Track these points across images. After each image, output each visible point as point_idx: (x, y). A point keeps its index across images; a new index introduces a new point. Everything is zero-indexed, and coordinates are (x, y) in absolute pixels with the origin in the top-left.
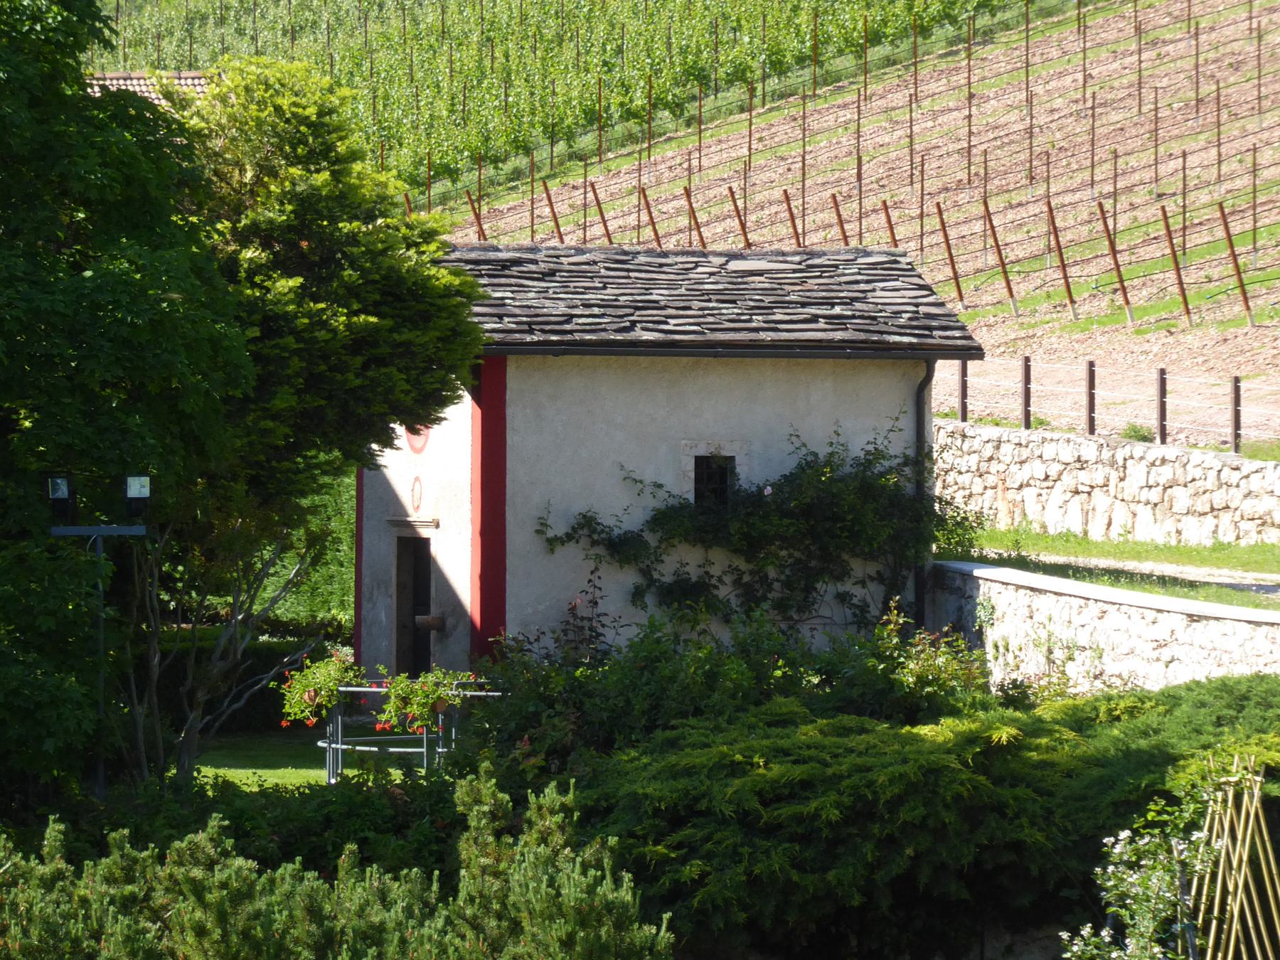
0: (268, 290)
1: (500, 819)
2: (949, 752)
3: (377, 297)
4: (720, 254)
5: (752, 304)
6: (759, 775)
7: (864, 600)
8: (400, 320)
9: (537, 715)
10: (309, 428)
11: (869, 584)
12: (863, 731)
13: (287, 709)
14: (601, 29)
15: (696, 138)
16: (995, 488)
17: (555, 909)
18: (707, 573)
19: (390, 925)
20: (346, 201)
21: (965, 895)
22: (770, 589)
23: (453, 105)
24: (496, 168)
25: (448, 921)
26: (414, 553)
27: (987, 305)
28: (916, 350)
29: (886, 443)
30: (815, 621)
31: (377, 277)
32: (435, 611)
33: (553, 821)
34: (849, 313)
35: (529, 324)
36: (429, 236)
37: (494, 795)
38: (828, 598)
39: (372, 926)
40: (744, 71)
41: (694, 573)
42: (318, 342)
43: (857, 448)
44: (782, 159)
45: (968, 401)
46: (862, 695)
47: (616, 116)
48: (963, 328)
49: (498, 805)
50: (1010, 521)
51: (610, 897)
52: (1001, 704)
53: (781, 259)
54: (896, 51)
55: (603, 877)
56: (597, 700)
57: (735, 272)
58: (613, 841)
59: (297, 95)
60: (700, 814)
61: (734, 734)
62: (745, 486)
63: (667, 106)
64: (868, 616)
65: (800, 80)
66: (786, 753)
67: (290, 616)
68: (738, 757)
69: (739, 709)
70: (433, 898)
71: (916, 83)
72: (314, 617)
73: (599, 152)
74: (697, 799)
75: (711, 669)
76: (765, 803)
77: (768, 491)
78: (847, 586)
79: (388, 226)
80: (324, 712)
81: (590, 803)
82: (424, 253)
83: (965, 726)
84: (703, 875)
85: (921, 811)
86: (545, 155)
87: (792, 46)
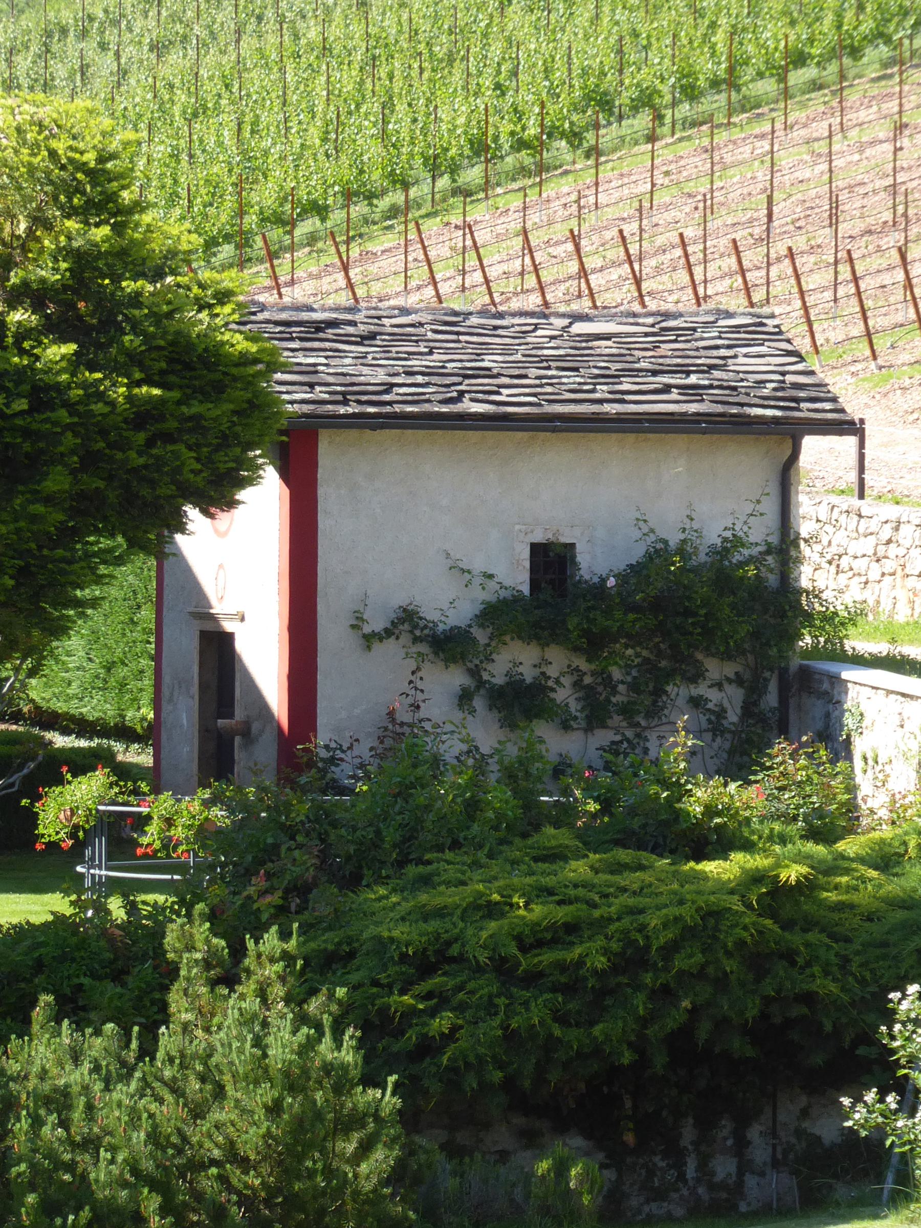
0: (38, 358)
1: (214, 967)
2: (732, 892)
3: (164, 365)
4: (563, 315)
5: (596, 371)
6: (518, 917)
7: (721, 705)
8: (189, 391)
9: (276, 846)
10: (87, 511)
11: (726, 686)
12: (641, 867)
13: (41, 830)
14: (496, 50)
15: (593, 171)
16: (893, 574)
17: (260, 1071)
18: (543, 674)
19: (76, 1089)
20: (129, 258)
21: (750, 1052)
22: (614, 692)
23: (327, 132)
24: (370, 204)
25: (145, 1083)
26: (218, 648)
27: (903, 365)
28: (779, 427)
29: (745, 529)
30: (664, 728)
31: (162, 343)
32: (239, 714)
33: (273, 970)
34: (706, 382)
35: (344, 394)
36: (223, 297)
37: (207, 941)
38: (681, 702)
39: (56, 1089)
40: (650, 96)
41: (528, 674)
42: (94, 416)
43: (713, 535)
44: (690, 195)
45: (866, 476)
46: (644, 826)
47: (506, 147)
48: (834, 400)
49: (212, 952)
50: (909, 612)
51: (329, 1057)
52: (802, 837)
53: (631, 320)
54: (825, 73)
55: (321, 1034)
56: (343, 832)
57: (579, 335)
58: (341, 992)
59: (74, 138)
60: (453, 960)
61: (495, 870)
62: (587, 577)
63: (563, 135)
64: (724, 722)
65: (715, 106)
66: (550, 892)
67: (96, 715)
68: (496, 897)
69: (502, 842)
70: (131, 1056)
71: (842, 111)
72: (123, 717)
73: (486, 186)
74: (449, 944)
75: (472, 797)
76: (523, 949)
77: (611, 582)
78: (702, 690)
79: (179, 285)
80: (81, 834)
81: (330, 947)
82: (217, 315)
83: (758, 862)
84: (454, 1029)
85: (699, 958)
86: (426, 191)
87: (706, 67)
